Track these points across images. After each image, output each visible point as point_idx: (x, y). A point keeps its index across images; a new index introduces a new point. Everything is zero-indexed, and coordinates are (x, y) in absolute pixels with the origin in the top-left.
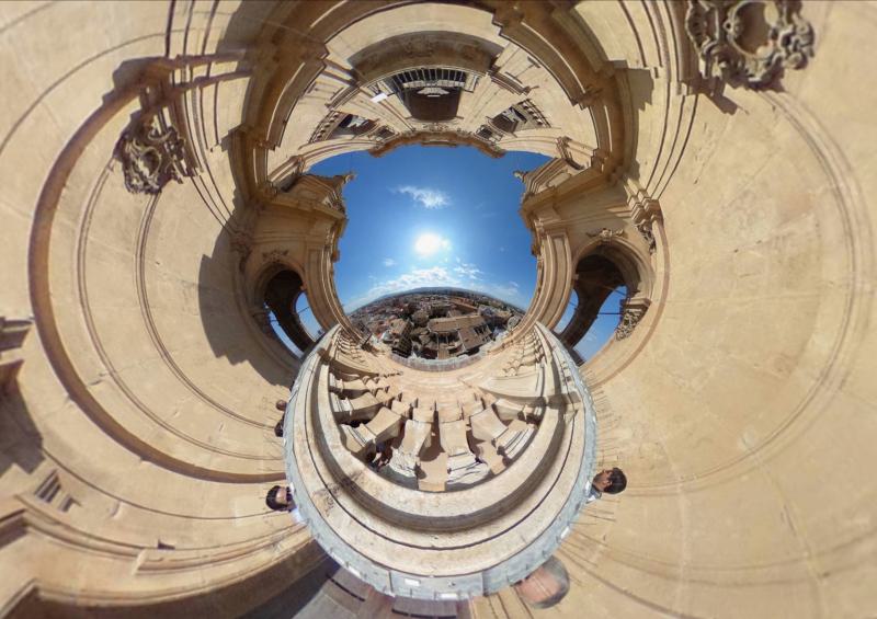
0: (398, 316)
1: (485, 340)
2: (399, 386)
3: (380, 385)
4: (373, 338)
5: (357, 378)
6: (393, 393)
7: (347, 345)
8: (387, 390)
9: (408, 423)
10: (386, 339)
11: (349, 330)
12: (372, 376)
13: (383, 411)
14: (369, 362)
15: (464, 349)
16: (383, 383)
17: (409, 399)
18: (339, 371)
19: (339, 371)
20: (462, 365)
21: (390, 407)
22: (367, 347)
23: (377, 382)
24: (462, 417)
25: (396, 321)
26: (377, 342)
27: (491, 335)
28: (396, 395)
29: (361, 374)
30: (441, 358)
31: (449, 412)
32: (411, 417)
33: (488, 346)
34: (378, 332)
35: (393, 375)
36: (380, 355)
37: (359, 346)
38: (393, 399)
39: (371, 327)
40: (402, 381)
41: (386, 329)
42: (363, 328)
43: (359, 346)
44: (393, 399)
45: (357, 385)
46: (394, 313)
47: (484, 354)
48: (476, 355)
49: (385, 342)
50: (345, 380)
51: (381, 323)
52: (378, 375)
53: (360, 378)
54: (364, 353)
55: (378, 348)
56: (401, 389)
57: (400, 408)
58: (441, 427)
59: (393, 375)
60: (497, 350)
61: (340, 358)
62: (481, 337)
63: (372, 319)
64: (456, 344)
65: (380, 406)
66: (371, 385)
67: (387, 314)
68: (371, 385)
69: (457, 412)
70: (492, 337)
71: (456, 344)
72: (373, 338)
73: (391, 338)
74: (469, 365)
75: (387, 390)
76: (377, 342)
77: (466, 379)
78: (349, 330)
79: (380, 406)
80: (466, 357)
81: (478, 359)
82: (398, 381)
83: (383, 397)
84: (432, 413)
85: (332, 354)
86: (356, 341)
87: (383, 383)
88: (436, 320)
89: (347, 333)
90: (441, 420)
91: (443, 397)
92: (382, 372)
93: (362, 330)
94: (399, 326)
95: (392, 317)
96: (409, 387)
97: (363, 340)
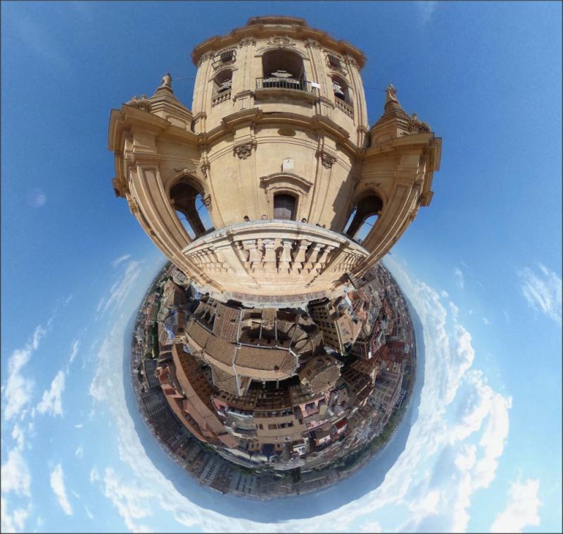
0: (365, 341)
1: (215, 304)
2: (303, 278)
3: (314, 270)
4: (351, 289)
5: (327, 261)
6: (305, 271)
7: (352, 262)
8: (309, 271)
9: (290, 260)
10: (343, 302)
11: (365, 264)
12: (322, 270)
13: (304, 260)
14: (334, 274)
15: (242, 312)
16: (314, 272)
17: (294, 272)
18: (335, 253)
19: (335, 253)
20: (252, 298)
21: (302, 263)
22: (345, 279)
23: (317, 270)
24: (265, 262)
25: (357, 330)
26: (346, 290)
27: (205, 301)
28: (302, 271)
29: (327, 265)
30: (273, 309)
31: (270, 267)
32: (290, 263)
33: (218, 296)
34: (355, 297)
35: (312, 282)
36: (331, 286)
37: (348, 271)
38: (303, 268)
39: (365, 291)
40: (304, 282)
41: (355, 309)
42: (366, 279)
43: (348, 271)
44: (303, 268)
45: (323, 259)
46: (374, 334)
47: (228, 294)
48: (234, 299)
49: (340, 298)
50: (329, 254)
51: (366, 306)
52: (320, 274)
53: (326, 263)
54: (340, 274)
55: (339, 288)
56: (301, 276)
57: (297, 265)
58: (275, 260)
59: (312, 282)
60: (216, 286)
61: (342, 255)
62: (214, 311)
63: (376, 294)
64: (249, 323)
65: (306, 261)
66: (318, 266)
67: (377, 322)
68: (318, 266)
69: (266, 266)
70: (206, 298)
71: (249, 323)
72: (351, 289)
73: (341, 308)
74: (246, 295)
75: (309, 271)
76: (346, 290)
77: (254, 285)
78: (365, 264)
79: (306, 261)
80: (245, 304)
81: (236, 294)
82: (305, 280)
83: (308, 266)
84: (280, 267)
85: (346, 250)
86: (354, 271)
87: (314, 272)
88: (280, 376)
89: (362, 263)
90: (275, 263)
91: (273, 277)
92: (320, 277)
93: (364, 279)
94: (348, 331)
95: (368, 328)
96: (297, 280)
97: (353, 277)
